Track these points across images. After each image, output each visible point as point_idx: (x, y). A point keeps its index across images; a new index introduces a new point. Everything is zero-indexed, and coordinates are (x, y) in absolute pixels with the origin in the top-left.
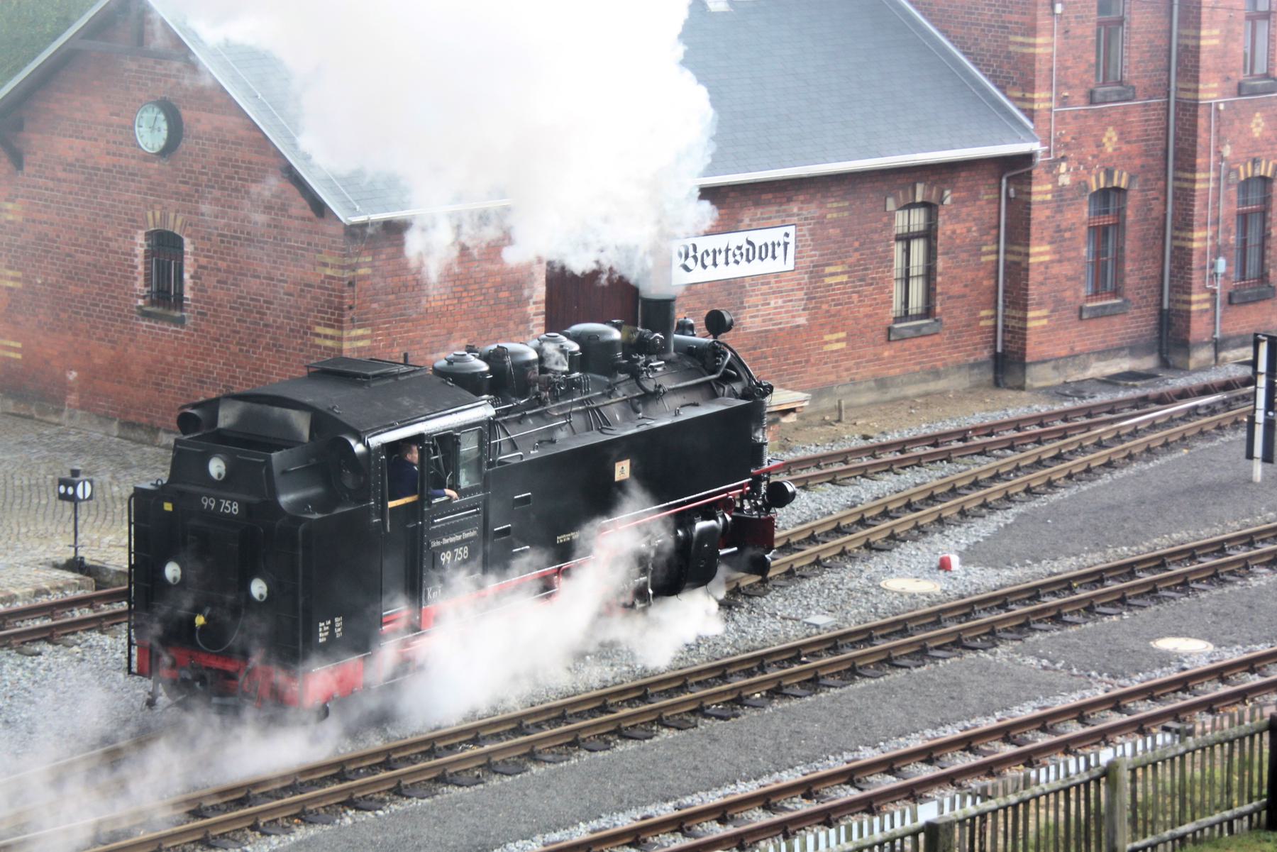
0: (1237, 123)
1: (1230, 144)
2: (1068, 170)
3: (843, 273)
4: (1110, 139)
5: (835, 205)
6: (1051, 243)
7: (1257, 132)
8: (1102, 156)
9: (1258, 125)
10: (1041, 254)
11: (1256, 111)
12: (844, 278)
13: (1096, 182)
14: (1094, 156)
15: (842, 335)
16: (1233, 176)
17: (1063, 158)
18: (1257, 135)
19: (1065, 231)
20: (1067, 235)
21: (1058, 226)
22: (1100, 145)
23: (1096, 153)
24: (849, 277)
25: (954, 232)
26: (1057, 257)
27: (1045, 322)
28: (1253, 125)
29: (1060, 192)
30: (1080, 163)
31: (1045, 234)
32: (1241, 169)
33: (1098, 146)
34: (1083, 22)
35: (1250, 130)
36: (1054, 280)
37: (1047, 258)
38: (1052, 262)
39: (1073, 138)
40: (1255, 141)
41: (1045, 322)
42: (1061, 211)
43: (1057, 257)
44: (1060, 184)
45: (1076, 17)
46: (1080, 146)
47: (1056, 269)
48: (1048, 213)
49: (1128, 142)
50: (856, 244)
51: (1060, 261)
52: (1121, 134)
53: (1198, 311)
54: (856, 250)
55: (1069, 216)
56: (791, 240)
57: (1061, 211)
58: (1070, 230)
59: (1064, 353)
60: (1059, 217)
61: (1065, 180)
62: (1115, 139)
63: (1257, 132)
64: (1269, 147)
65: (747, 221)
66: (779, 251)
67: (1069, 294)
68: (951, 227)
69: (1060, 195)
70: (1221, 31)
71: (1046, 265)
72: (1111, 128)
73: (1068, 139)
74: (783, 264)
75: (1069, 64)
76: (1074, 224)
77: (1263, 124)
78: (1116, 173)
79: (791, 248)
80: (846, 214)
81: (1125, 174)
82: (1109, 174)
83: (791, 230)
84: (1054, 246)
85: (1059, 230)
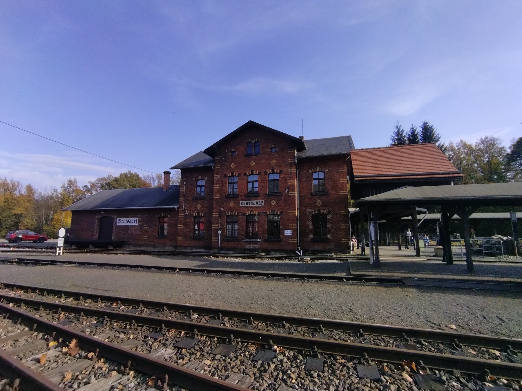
4: (199, 207)
6: (183, 225)
9: (232, 204)
16: (223, 214)
17: (186, 210)
18: (232, 206)
29: (186, 216)
40: (231, 207)
47: (185, 230)
48: (183, 219)
56: (138, 220)
59: (187, 246)
60: (185, 220)
65: (130, 217)
66: (135, 222)
73: (188, 206)
74: (136, 224)
77: (230, 204)
79: (138, 222)
82: (198, 213)
83: (138, 219)
85: (185, 222)
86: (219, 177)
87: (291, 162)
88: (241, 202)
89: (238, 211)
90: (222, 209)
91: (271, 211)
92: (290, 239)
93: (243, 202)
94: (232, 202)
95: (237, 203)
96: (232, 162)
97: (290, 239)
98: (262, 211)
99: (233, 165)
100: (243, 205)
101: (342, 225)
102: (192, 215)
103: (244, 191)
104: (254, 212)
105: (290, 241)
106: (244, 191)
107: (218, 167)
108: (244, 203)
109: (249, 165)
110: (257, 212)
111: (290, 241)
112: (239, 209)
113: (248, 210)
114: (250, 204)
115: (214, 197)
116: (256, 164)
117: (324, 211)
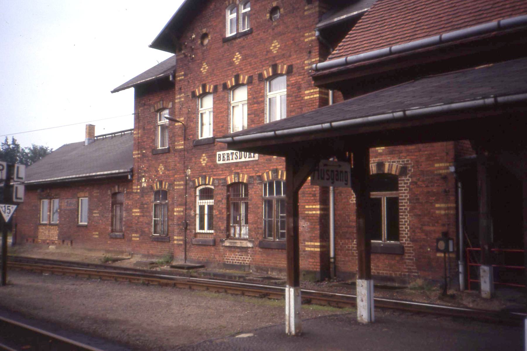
0: (194, 159)
1: (190, 169)
2: (145, 181)
3: (98, 213)
4: (161, 169)
5: (96, 191)
6: (139, 209)
7: (204, 163)
8: (158, 176)
9: (204, 160)
10: (136, 212)
11: (203, 153)
12: (98, 215)
13: (156, 186)
14: (155, 176)
15: (97, 233)
17: (143, 176)
18: (204, 165)
19: (145, 205)
20: (145, 206)
21: (142, 202)
22: (157, 171)
23: (155, 174)
24: (99, 215)
25: (128, 203)
26: (142, 214)
27: (138, 239)
28: (202, 160)
29: (143, 189)
30: (150, 179)
31: (138, 205)
32: (196, 180)
33: (156, 172)
34: (150, 124)
35: (200, 162)
36: (141, 223)
37: (138, 214)
38: (140, 216)
39: (147, 169)
40: (203, 168)
41: (138, 239)
42: (143, 197)
43: (142, 214)
44: (142, 186)
45: (148, 122)
46: (149, 171)
48: (138, 197)
49: (168, 170)
50: (101, 204)
51: (143, 216)
52: (165, 167)
53: (177, 244)
54: (101, 206)
55: (146, 199)
57: (143, 197)
58: (146, 204)
61: (144, 185)
62: (163, 169)
63: (204, 163)
64: (210, 170)
67: (146, 229)
68: (127, 201)
69: (143, 191)
70: (185, 118)
71: (138, 217)
72: (161, 165)
75: (145, 140)
76: (148, 202)
77: (202, 160)
78: (164, 183)
80: (98, 194)
81: (167, 183)
84: (141, 210)
85: (143, 204)
86: (183, 99)
87: (310, 39)
88: (218, 153)
89: (214, 175)
90: (189, 172)
91: (270, 173)
92: (307, 243)
93: (221, 153)
94: (204, 155)
95: (212, 157)
96: (204, 59)
97: (307, 243)
98: (254, 174)
99: (205, 68)
100: (221, 162)
101: (437, 205)
102: (152, 188)
103: (222, 127)
104: (241, 176)
105: (307, 249)
106: (222, 127)
107: (182, 76)
108: (223, 157)
109: (232, 63)
110: (246, 176)
111: (307, 249)
112: (215, 170)
113: (231, 173)
114: (234, 156)
115: (177, 145)
116: (245, 58)
117: (391, 167)
